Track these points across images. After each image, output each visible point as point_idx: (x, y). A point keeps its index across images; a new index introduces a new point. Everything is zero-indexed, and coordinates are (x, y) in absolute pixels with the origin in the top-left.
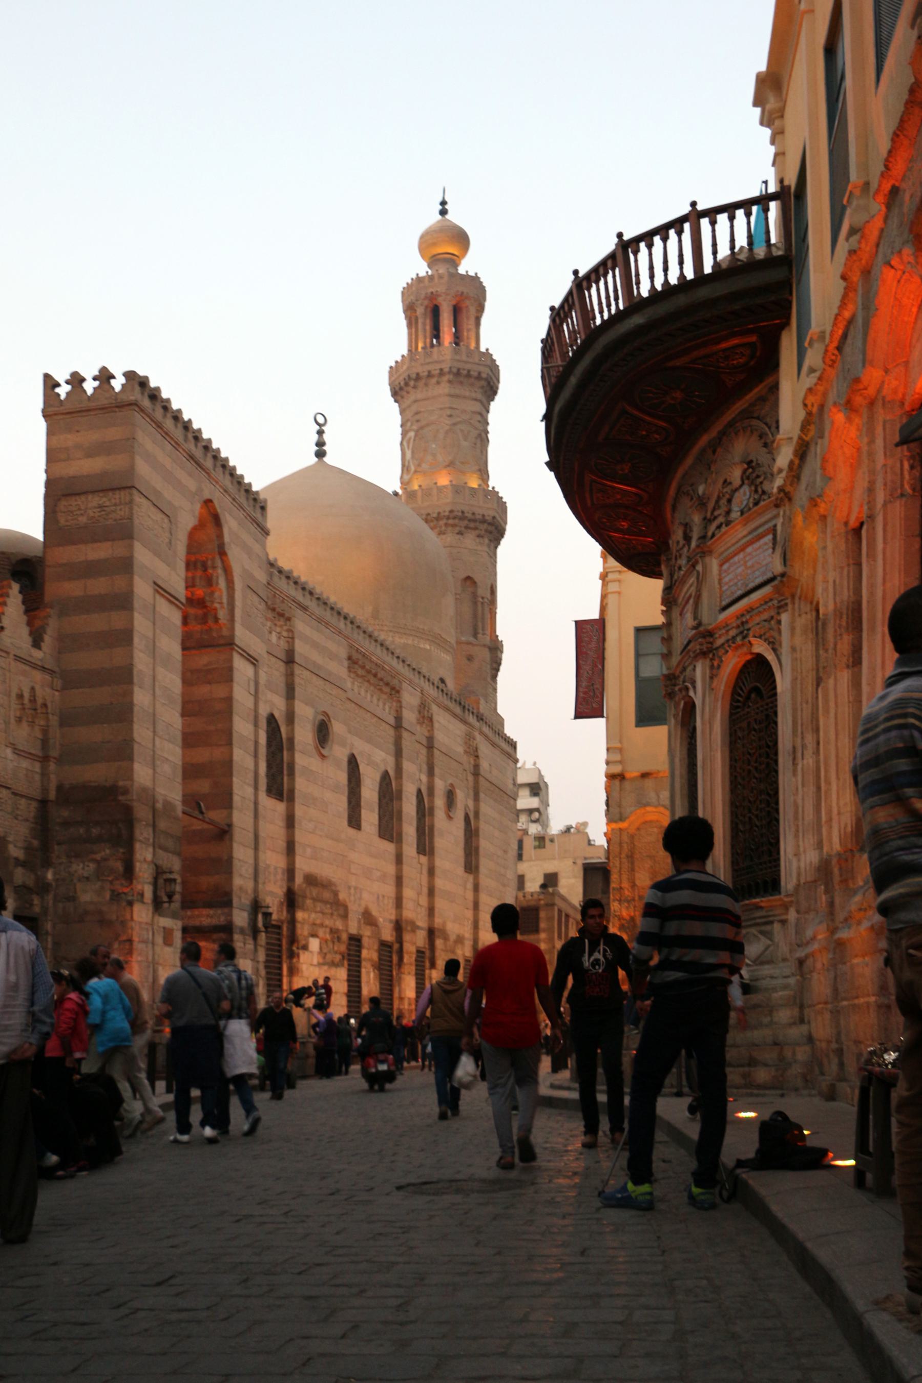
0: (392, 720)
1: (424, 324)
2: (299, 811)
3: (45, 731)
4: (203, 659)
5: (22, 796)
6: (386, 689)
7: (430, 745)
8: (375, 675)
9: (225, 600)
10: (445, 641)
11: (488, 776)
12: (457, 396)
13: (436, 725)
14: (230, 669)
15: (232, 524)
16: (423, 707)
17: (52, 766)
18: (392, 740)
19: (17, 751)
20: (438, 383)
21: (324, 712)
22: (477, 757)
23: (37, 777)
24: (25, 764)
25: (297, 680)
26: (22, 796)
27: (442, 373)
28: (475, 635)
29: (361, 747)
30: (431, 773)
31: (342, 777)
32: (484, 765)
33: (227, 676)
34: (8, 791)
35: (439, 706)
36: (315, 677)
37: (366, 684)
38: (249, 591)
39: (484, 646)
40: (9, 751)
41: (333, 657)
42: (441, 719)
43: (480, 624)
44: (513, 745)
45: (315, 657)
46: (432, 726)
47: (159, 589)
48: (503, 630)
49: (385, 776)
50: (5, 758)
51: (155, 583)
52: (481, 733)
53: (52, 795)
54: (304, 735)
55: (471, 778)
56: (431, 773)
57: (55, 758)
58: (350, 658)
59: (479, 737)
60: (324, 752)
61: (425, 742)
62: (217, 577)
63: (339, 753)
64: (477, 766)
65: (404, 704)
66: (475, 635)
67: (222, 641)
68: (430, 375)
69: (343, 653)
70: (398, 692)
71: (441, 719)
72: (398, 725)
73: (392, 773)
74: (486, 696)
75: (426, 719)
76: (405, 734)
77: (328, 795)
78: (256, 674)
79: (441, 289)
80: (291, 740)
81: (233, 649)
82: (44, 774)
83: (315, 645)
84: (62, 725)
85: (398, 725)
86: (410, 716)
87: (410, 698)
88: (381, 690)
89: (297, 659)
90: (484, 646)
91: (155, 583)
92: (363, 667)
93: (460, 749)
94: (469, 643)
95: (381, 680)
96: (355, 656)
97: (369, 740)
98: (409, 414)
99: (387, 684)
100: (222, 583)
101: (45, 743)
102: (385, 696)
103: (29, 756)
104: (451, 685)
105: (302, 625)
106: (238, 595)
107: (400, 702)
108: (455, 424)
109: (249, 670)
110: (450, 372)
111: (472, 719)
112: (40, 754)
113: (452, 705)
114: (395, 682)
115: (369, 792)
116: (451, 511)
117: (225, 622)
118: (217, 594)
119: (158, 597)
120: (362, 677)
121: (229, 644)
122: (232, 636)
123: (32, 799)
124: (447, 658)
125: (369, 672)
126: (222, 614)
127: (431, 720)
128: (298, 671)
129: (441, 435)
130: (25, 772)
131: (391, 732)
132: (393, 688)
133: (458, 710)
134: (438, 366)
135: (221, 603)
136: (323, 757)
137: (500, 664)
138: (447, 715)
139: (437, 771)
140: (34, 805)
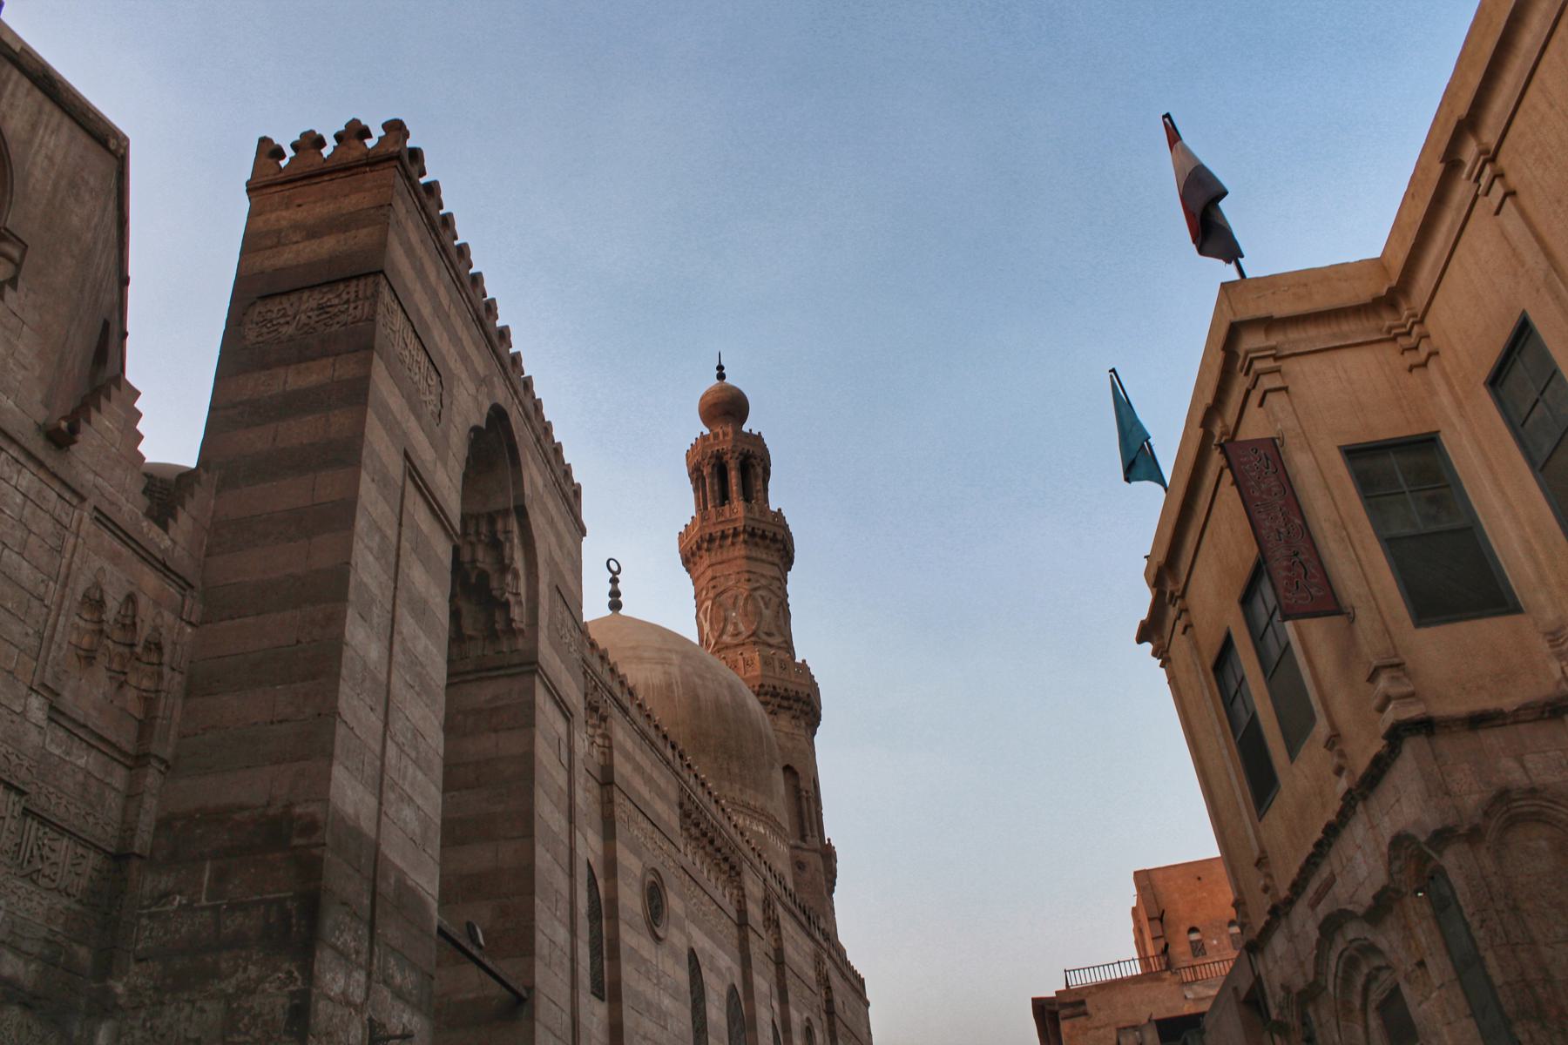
0: (734, 915)
1: (712, 485)
2: (629, 1019)
3: (149, 702)
4: (482, 694)
5: (62, 831)
6: (725, 867)
7: (779, 961)
8: (712, 842)
9: (522, 590)
10: (782, 828)
11: (841, 1014)
12: (756, 559)
13: (784, 932)
14: (531, 705)
15: (534, 475)
16: (767, 904)
17: (152, 778)
18: (735, 942)
19: (56, 713)
20: (733, 544)
21: (654, 869)
22: (829, 988)
23: (114, 801)
24: (84, 759)
25: (618, 812)
26: (62, 831)
27: (736, 534)
28: (803, 838)
29: (702, 943)
30: (784, 1001)
31: (682, 976)
32: (838, 1000)
33: (526, 718)
34: (13, 797)
35: (784, 905)
36: (641, 817)
37: (701, 852)
38: (557, 596)
39: (815, 851)
40: (35, 703)
41: (662, 795)
42: (788, 926)
43: (807, 825)
44: (862, 982)
45: (638, 783)
46: (779, 933)
47: (413, 471)
48: (834, 829)
49: (732, 990)
50: (23, 714)
51: (407, 456)
52: (830, 956)
53: (143, 839)
54: (631, 900)
55: (824, 1017)
56: (784, 1001)
57: (163, 761)
58: (681, 805)
59: (828, 961)
60: (661, 934)
61: (772, 954)
62: (512, 548)
63: (676, 938)
64: (829, 1001)
65: (747, 892)
66: (803, 838)
67: (516, 660)
68: (724, 536)
69: (673, 795)
70: (739, 874)
71: (788, 926)
72: (742, 923)
73: (740, 990)
74: (825, 917)
75: (773, 923)
76: (752, 936)
77: (667, 1002)
78: (570, 735)
79: (727, 446)
80: (613, 901)
81: (535, 672)
82: (132, 795)
83: (638, 768)
84: (189, 693)
85: (742, 923)
86: (755, 912)
87: (754, 888)
88: (718, 865)
89: (617, 779)
90: (815, 851)
91: (407, 456)
92: (697, 825)
93: (812, 974)
94: (797, 847)
95: (719, 850)
96: (688, 806)
97: (710, 934)
98: (703, 582)
99: (726, 859)
100: (519, 563)
101: (145, 727)
102: (724, 877)
103: (98, 742)
104: (790, 885)
105: (621, 733)
106: (543, 588)
107: (741, 889)
108: (755, 589)
109: (561, 726)
110: (744, 531)
111: (818, 936)
112: (129, 748)
113: (797, 912)
114: (734, 859)
115: (716, 1013)
116: (761, 686)
117: (523, 626)
118: (509, 578)
119: (409, 483)
120: (696, 839)
121: (530, 666)
122: (535, 651)
123: (86, 844)
124: (784, 849)
125: (704, 834)
126: (517, 613)
127: (778, 926)
128: (618, 798)
129: (741, 603)
130: (80, 777)
131: (735, 931)
132: (732, 868)
133: (803, 919)
134: (731, 526)
135: (517, 594)
136: (658, 939)
137: (835, 876)
138: (794, 924)
139: (791, 997)
140: (93, 859)
